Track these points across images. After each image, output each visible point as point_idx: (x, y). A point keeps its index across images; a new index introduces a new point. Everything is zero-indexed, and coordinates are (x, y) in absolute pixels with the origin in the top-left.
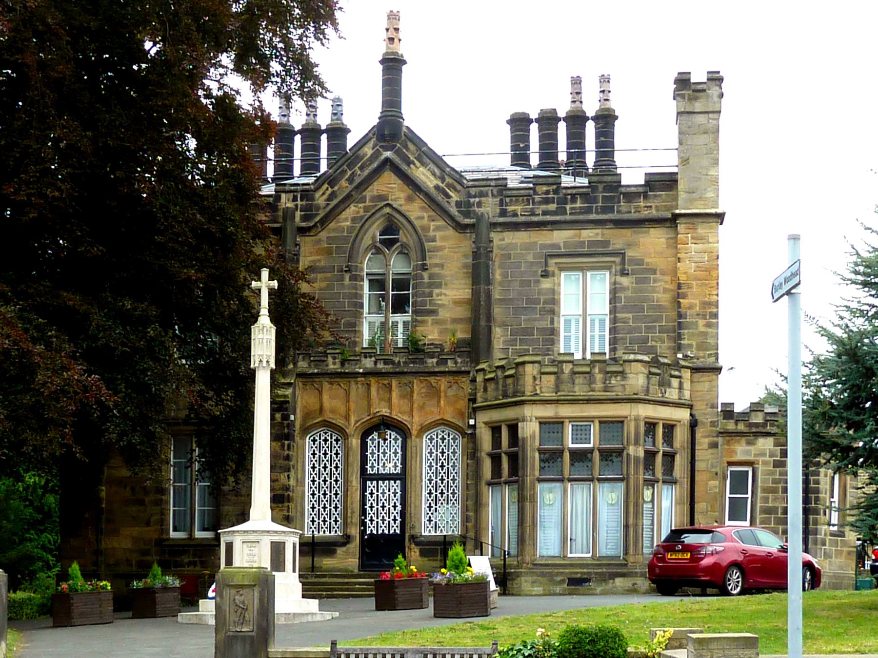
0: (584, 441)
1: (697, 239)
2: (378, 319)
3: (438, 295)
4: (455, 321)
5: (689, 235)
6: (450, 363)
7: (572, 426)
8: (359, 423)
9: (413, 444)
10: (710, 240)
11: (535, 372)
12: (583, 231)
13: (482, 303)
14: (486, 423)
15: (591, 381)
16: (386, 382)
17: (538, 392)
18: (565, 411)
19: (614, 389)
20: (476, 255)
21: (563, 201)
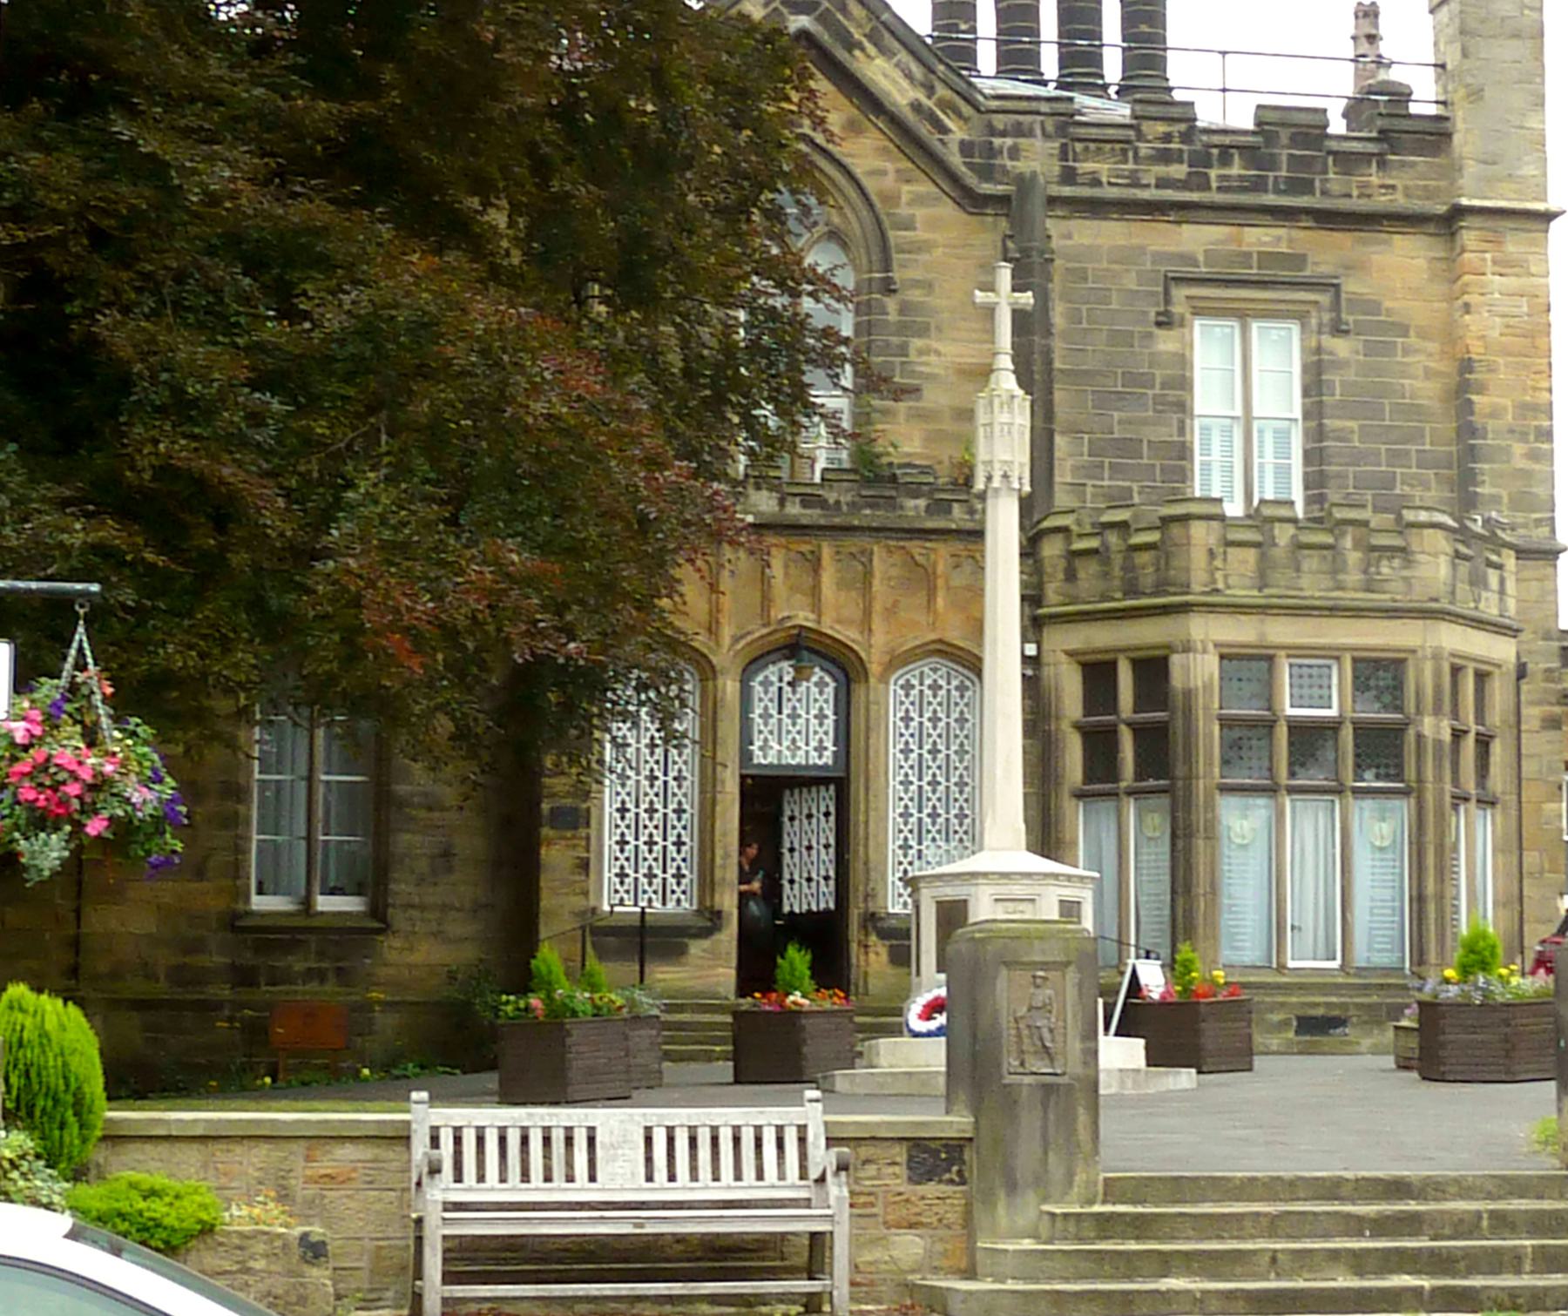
0: (1316, 702)
1: (1505, 266)
3: (921, 353)
5: (1488, 256)
6: (957, 510)
7: (1291, 666)
8: (742, 643)
10: (1533, 269)
11: (1213, 540)
12: (1247, 229)
13: (1037, 377)
14: (1070, 654)
15: (1336, 568)
16: (805, 548)
17: (1220, 585)
18: (1281, 631)
19: (1387, 586)
21: (1201, 160)
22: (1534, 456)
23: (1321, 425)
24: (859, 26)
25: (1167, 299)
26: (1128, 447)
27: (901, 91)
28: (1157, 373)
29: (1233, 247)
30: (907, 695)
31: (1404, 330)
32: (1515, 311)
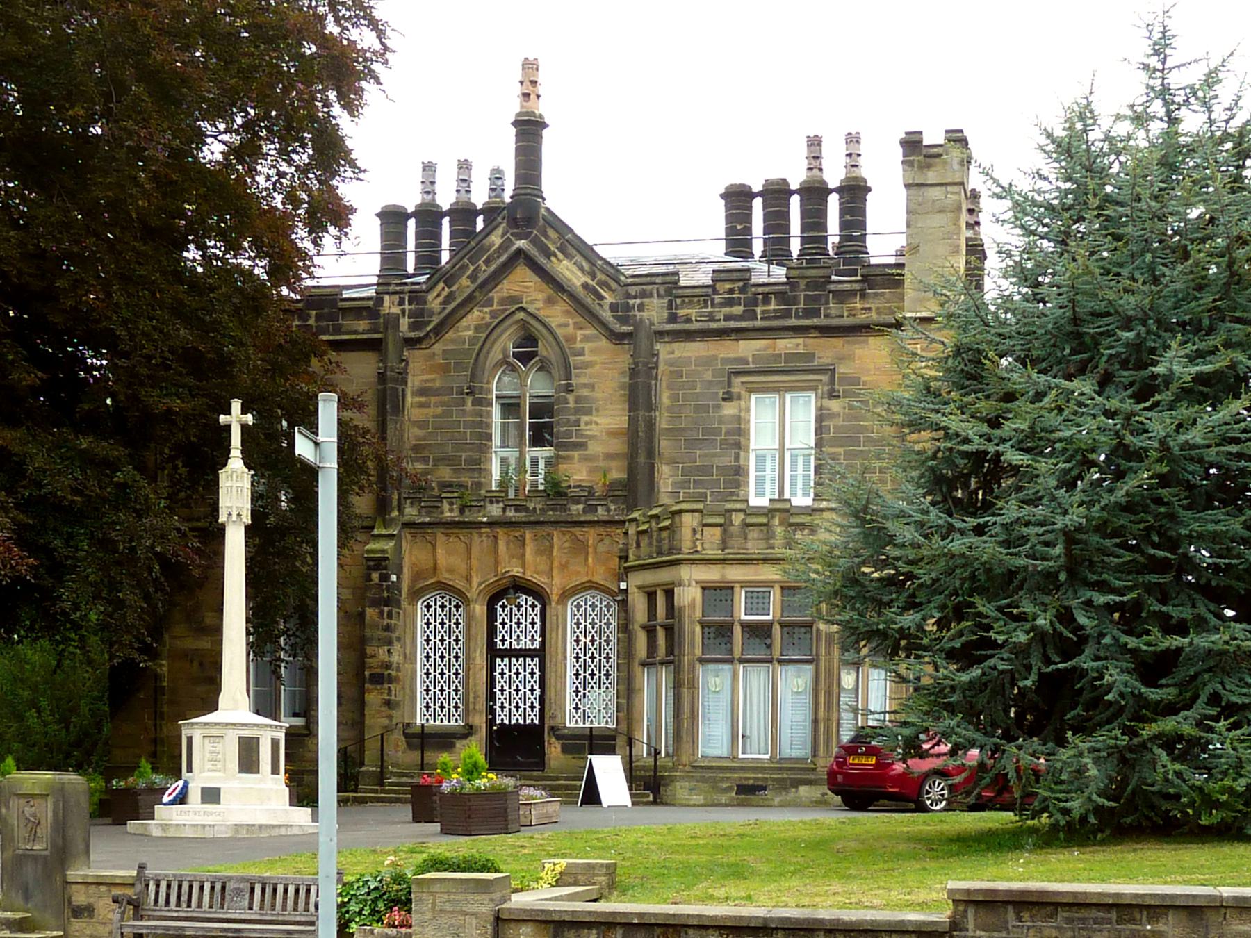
2: (512, 453)
3: (587, 424)
4: (609, 456)
5: (919, 346)
6: (600, 510)
7: (746, 592)
9: (554, 612)
13: (641, 434)
14: (639, 588)
15: (770, 535)
16: (517, 534)
17: (699, 549)
18: (735, 573)
20: (633, 373)
24: (554, 243)
25: (729, 384)
26: (705, 470)
27: (578, 278)
28: (723, 427)
29: (770, 351)
30: (578, 611)
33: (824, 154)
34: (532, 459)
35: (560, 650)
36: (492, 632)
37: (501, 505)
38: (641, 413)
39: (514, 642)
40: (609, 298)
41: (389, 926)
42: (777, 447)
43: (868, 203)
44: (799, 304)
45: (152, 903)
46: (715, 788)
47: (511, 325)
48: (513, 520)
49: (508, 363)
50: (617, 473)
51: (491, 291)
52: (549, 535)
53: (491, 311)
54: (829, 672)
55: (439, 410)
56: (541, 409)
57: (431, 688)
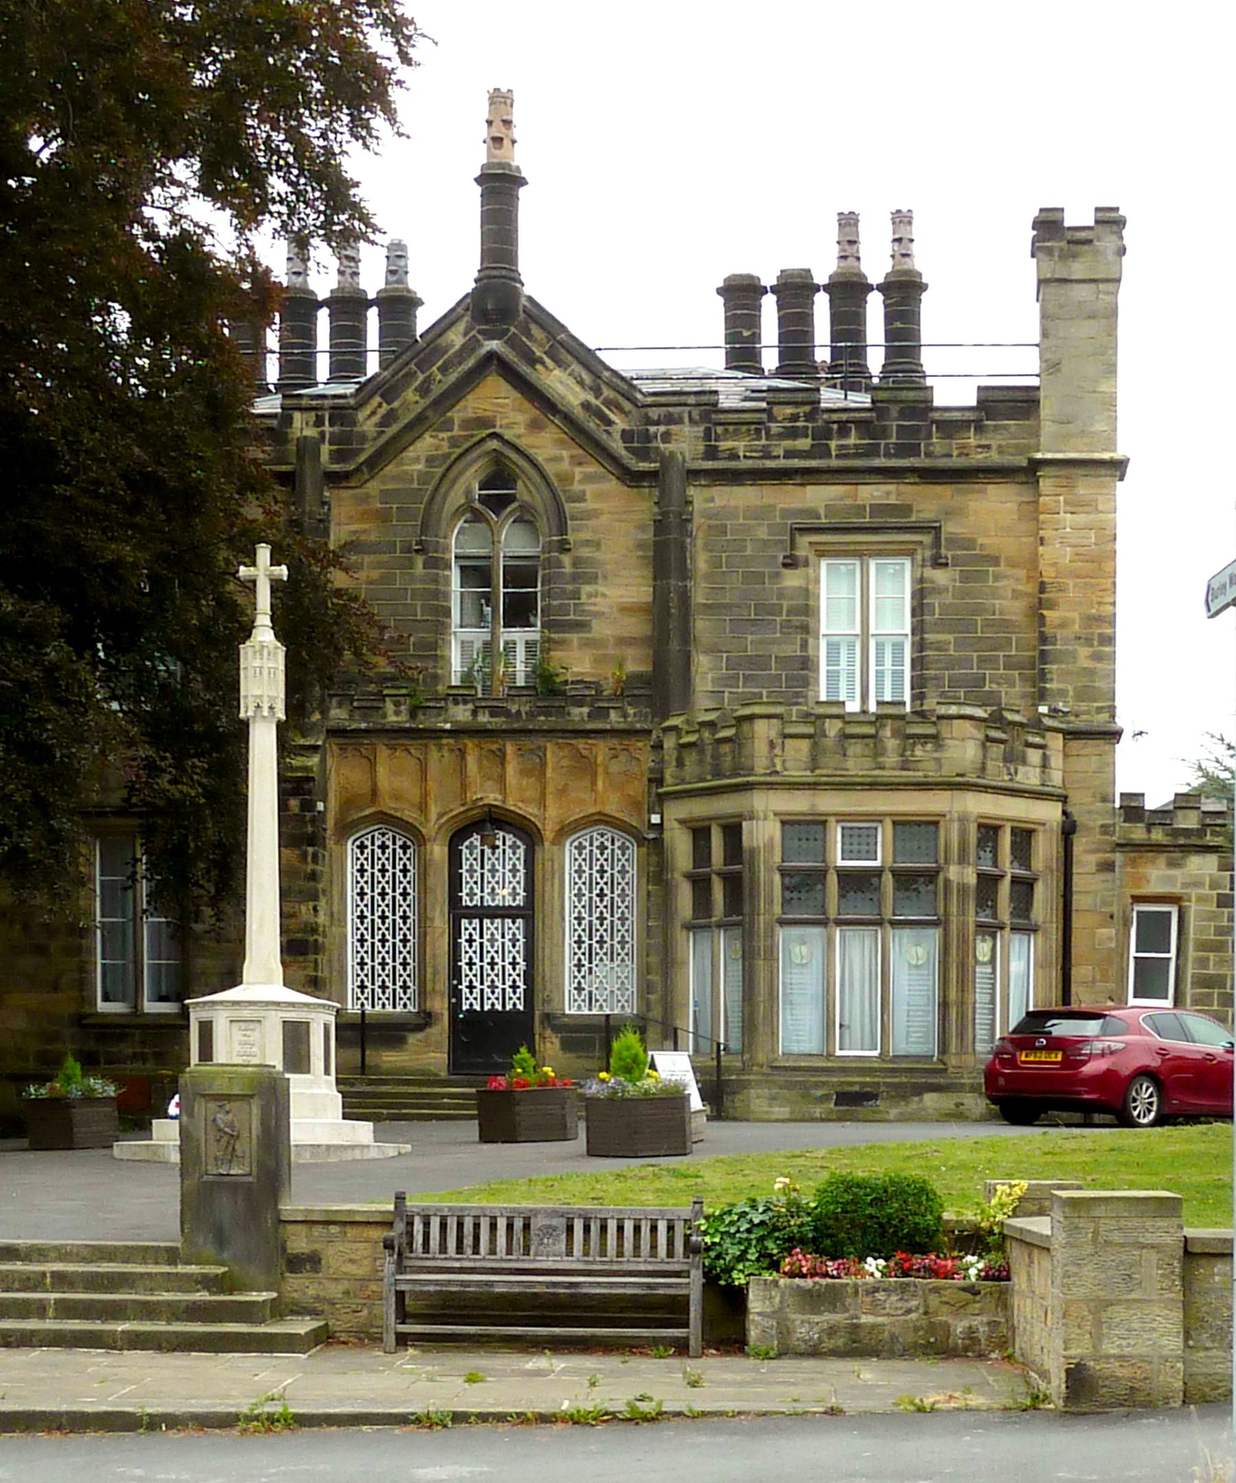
0: (864, 855)
2: (478, 636)
3: (590, 596)
4: (622, 641)
6: (613, 715)
7: (843, 828)
8: (445, 818)
9: (547, 856)
11: (773, 734)
12: (860, 487)
13: (673, 611)
14: (682, 822)
16: (494, 747)
17: (779, 768)
18: (829, 802)
19: (920, 765)
20: (660, 526)
21: (823, 434)
22: (1098, 657)
23: (922, 639)
25: (793, 545)
26: (760, 662)
29: (849, 502)
30: (580, 854)
31: (995, 561)
32: (1086, 542)
33: (862, 238)
34: (506, 643)
35: (556, 911)
36: (455, 883)
37: (470, 706)
38: (673, 582)
39: (487, 897)
40: (620, 423)
41: (791, 1275)
42: (858, 631)
43: (923, 306)
44: (891, 437)
45: (420, 1249)
46: (806, 1096)
47: (479, 457)
48: (489, 727)
49: (474, 511)
50: (636, 663)
51: (450, 410)
52: (539, 748)
53: (450, 438)
54: (963, 940)
55: (375, 574)
56: (520, 574)
57: (368, 960)
